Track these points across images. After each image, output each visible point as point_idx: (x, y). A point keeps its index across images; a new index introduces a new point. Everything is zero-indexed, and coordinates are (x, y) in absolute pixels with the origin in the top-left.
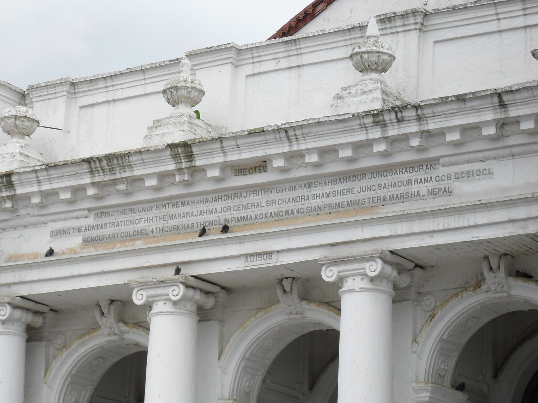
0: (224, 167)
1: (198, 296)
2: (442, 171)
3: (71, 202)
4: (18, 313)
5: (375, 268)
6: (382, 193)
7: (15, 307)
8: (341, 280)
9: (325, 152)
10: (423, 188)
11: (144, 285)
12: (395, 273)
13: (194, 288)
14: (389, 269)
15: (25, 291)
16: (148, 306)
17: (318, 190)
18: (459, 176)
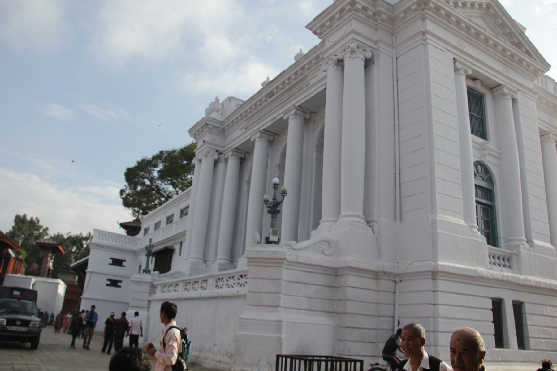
0: (266, 96)
1: (266, 136)
2: (308, 79)
3: (241, 119)
4: (235, 153)
5: (293, 111)
6: (296, 91)
7: (233, 151)
8: (288, 118)
9: (283, 83)
10: (304, 86)
11: (253, 135)
12: (302, 113)
13: (265, 134)
14: (299, 112)
15: (235, 146)
16: (255, 140)
17: (285, 96)
18: (311, 79)
